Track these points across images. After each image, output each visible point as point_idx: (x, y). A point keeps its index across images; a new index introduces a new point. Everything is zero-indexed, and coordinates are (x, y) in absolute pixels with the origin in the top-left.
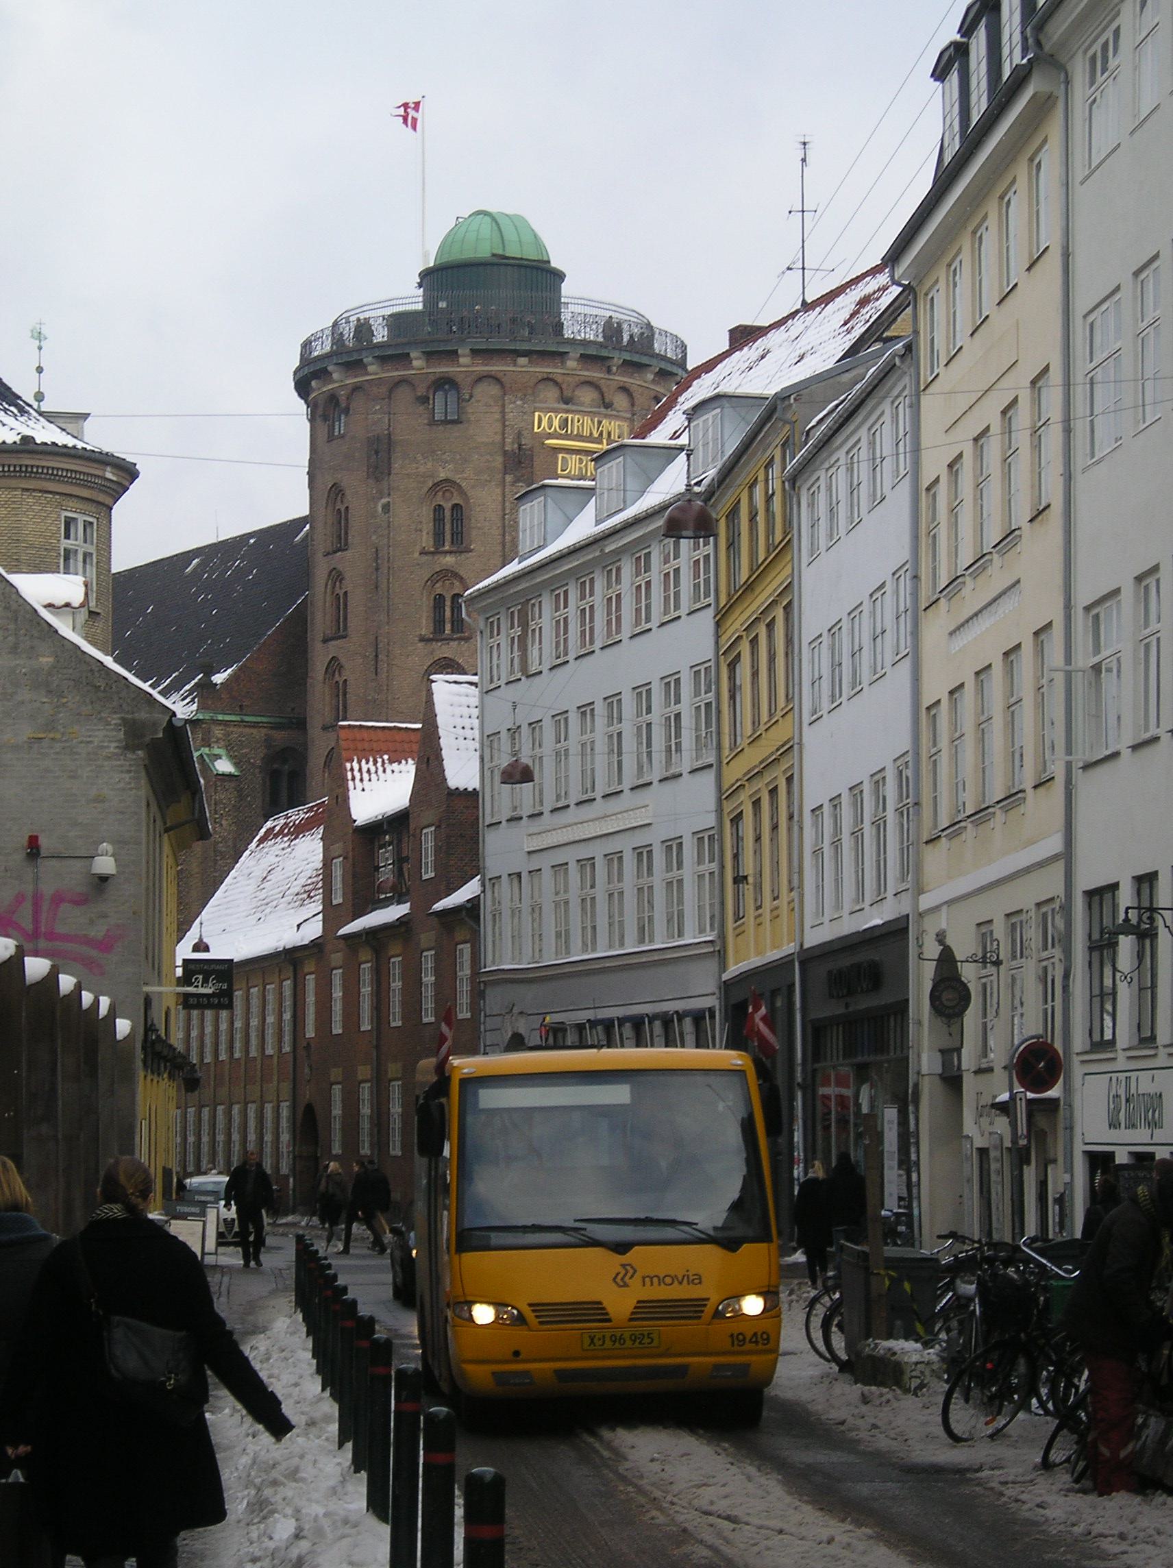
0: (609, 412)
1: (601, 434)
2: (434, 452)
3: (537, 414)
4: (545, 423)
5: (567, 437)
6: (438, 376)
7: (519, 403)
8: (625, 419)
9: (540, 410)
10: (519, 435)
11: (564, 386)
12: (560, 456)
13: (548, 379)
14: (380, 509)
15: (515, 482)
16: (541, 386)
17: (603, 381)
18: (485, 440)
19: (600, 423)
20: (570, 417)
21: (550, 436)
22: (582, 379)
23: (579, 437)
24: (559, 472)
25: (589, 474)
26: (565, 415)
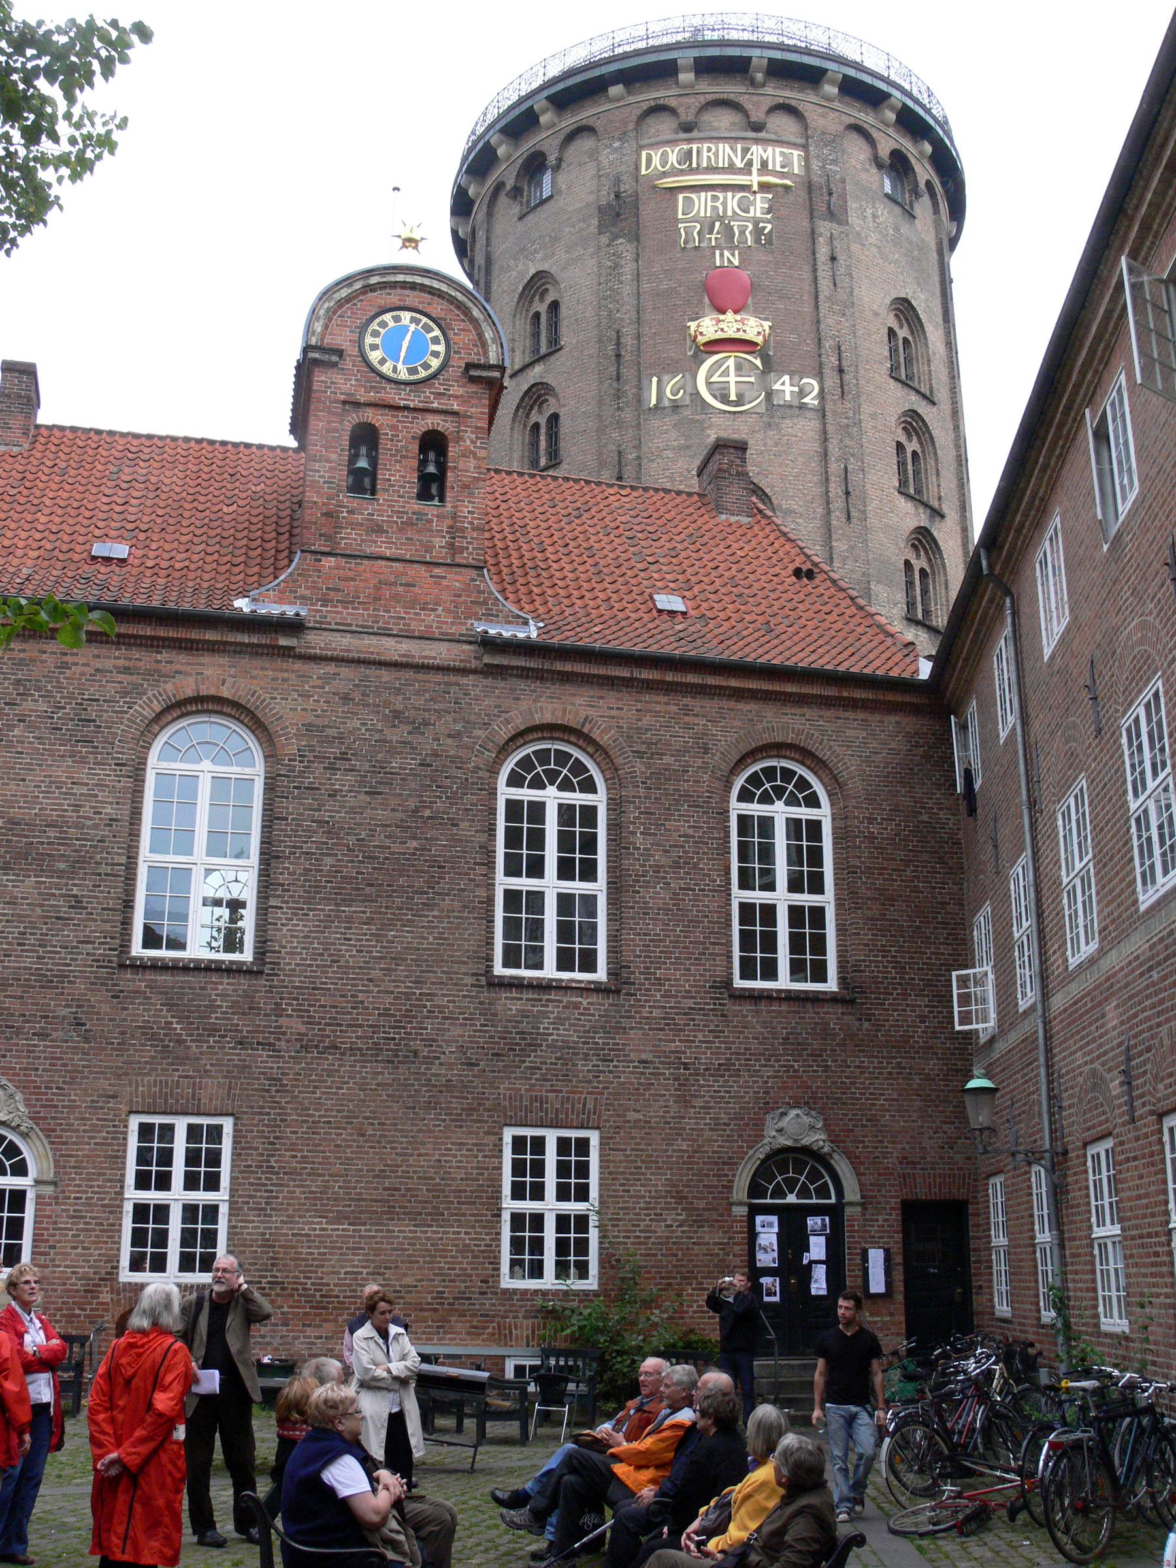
0: (762, 135)
1: (750, 164)
2: (524, 248)
3: (644, 154)
4: (656, 160)
5: (691, 171)
8: (794, 145)
9: (651, 146)
12: (681, 197)
15: (613, 240)
16: (650, 120)
17: (747, 96)
18: (578, 205)
19: (745, 151)
20: (695, 147)
21: (664, 174)
22: (710, 97)
24: (680, 216)
25: (730, 213)
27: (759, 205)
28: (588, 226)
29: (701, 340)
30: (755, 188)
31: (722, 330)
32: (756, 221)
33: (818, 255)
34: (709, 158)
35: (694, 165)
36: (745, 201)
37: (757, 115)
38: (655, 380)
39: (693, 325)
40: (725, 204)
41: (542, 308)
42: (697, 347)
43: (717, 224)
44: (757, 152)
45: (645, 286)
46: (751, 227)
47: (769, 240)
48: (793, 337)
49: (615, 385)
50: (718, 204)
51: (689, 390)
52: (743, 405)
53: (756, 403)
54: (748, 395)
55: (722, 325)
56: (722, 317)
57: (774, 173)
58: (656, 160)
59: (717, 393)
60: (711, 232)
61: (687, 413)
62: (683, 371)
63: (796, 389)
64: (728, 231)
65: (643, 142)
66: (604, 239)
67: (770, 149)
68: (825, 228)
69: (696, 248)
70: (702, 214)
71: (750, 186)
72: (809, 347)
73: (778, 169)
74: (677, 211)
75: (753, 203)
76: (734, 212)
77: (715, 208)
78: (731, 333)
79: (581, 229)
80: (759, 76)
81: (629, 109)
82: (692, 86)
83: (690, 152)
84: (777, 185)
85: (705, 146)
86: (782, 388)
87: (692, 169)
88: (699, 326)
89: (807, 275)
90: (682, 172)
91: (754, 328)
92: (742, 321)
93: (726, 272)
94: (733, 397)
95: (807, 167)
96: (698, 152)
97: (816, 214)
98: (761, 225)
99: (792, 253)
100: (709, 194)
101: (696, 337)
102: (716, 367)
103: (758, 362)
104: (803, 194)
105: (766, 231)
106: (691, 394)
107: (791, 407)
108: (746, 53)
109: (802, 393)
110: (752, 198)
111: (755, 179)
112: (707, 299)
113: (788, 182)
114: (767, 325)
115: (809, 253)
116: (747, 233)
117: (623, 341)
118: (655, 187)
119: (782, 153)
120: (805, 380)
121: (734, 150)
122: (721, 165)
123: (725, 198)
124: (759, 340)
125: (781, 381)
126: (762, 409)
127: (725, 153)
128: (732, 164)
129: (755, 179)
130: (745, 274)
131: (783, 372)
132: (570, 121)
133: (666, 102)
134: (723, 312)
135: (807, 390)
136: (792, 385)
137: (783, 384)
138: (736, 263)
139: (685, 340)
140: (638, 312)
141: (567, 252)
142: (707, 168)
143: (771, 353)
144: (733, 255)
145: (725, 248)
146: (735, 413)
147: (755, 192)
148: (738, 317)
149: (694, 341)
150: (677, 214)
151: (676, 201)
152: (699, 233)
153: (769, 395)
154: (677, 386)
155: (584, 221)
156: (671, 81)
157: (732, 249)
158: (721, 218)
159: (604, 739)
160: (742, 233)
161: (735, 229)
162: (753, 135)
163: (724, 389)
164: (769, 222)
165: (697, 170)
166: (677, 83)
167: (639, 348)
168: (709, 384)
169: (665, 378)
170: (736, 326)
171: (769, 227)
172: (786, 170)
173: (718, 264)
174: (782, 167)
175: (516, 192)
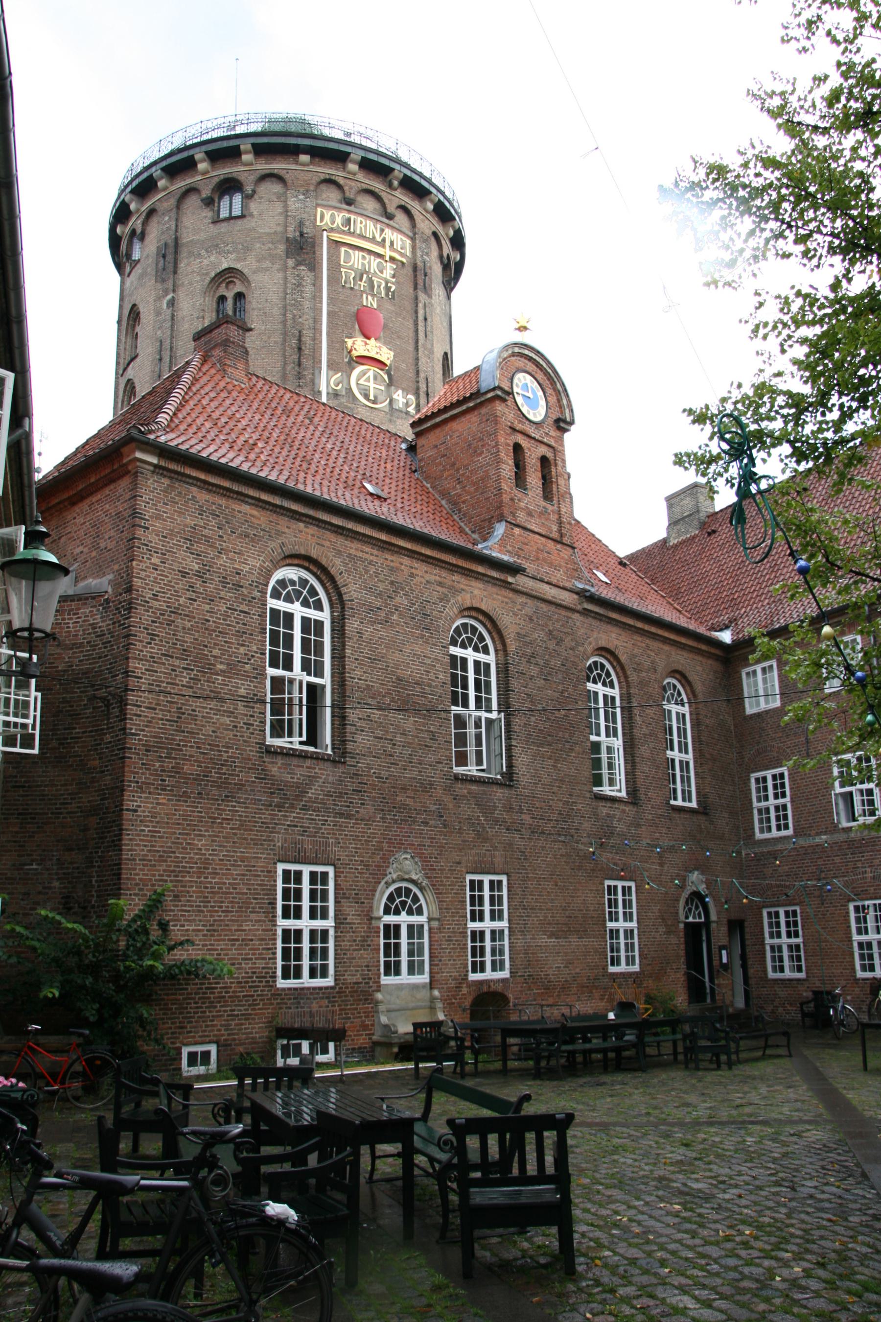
0: (391, 223)
2: (217, 245)
3: (319, 210)
5: (350, 233)
6: (222, 177)
7: (301, 197)
10: (301, 224)
11: (346, 188)
13: (330, 182)
14: (165, 306)
16: (323, 187)
18: (268, 230)
20: (353, 217)
22: (365, 186)
23: (362, 237)
26: (347, 215)
28: (276, 248)
29: (355, 353)
30: (387, 259)
37: (350, 194)
39: (349, 342)
40: (369, 263)
41: (230, 295)
42: (351, 358)
44: (389, 234)
49: (297, 368)
53: (383, 405)
55: (368, 347)
60: (361, 280)
61: (343, 400)
64: (371, 282)
65: (320, 202)
66: (291, 263)
68: (422, 297)
69: (352, 289)
72: (411, 374)
75: (385, 268)
77: (363, 264)
78: (372, 354)
79: (269, 249)
80: (396, 183)
81: (311, 175)
82: (355, 174)
83: (349, 220)
89: (410, 324)
90: (343, 232)
91: (386, 355)
103: (386, 377)
108: (393, 165)
111: (388, 253)
112: (357, 326)
113: (404, 260)
117: (303, 339)
124: (388, 363)
126: (387, 410)
127: (370, 228)
128: (374, 238)
132: (264, 166)
133: (337, 178)
134: (369, 338)
138: (375, 306)
141: (258, 261)
155: (273, 243)
156: (340, 166)
157: (373, 296)
159: (623, 658)
160: (379, 287)
162: (386, 221)
165: (352, 234)
166: (344, 168)
175: (209, 202)
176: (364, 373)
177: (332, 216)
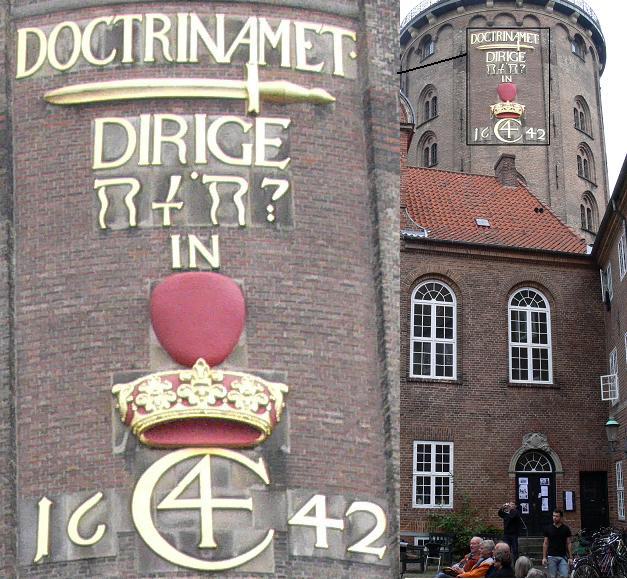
1: (243, 54)
3: (22, 34)
4: (48, 49)
5: (121, 70)
8: (336, 17)
9: (37, 17)
12: (99, 124)
19: (234, 28)
20: (128, 20)
21: (65, 77)
24: (98, 164)
25: (201, 158)
27: (261, 140)
29: (141, 421)
30: (254, 105)
31: (185, 400)
32: (256, 175)
33: (384, 245)
34: (158, 42)
35: (127, 58)
36: (233, 134)
38: (45, 505)
39: (124, 391)
40: (190, 139)
42: (134, 437)
43: (175, 181)
44: (258, 30)
45: (26, 310)
46: (244, 186)
47: (283, 216)
48: (334, 417)
50: (177, 139)
51: (117, 525)
52: (229, 557)
53: (257, 551)
54: (239, 536)
55: (185, 391)
56: (184, 374)
57: (294, 74)
58: (48, 49)
59: (175, 533)
60: (162, 198)
62: (104, 487)
63: (339, 524)
64: (198, 194)
65: (20, 10)
67: (285, 25)
70: (144, 160)
71: (243, 102)
73: (302, 65)
74: (91, 152)
75: (250, 137)
76: (210, 155)
77: (170, 147)
78: (203, 408)
83: (118, 30)
84: (299, 100)
85: (150, 17)
86: (309, 521)
87: (123, 67)
88: (136, 392)
90: (101, 73)
92: (227, 383)
93: (193, 278)
94: (208, 541)
95: (363, 61)
96: (135, 30)
97: (380, 159)
98: (266, 182)
99: (330, 241)
100: (159, 118)
101: (130, 416)
102: (171, 477)
103: (260, 468)
104: (354, 118)
105: (276, 196)
106: (121, 535)
107: (328, 561)
109: (351, 533)
110: (247, 126)
111: (252, 87)
112: (153, 337)
114: (278, 389)
115: (367, 240)
116: (237, 198)
118: (46, 103)
119: (310, 33)
120: (356, 506)
121: (211, 27)
122: (182, 58)
123: (192, 127)
124: (263, 421)
125: (307, 507)
126: (269, 566)
128: (205, 57)
129: (252, 87)
130: (233, 285)
131: (314, 488)
134: (188, 364)
135: (362, 524)
136: (330, 515)
137: (312, 513)
138: (215, 262)
139: (107, 421)
140: (11, 365)
142: (153, 64)
143: (287, 449)
144: (208, 245)
145: (192, 230)
146: (211, 573)
147: (253, 114)
148: (219, 374)
149: (127, 423)
150: (90, 159)
151: (89, 133)
152: (137, 199)
153: (284, 536)
154: (92, 518)
157: (205, 233)
158: (181, 169)
160: (227, 199)
161: (213, 190)
163: (190, 523)
164: (282, 175)
165: (133, 69)
167: (12, 440)
168: (157, 513)
169: (67, 500)
170: (217, 391)
171: (283, 186)
172: (317, 68)
173: (176, 264)
174: (311, 61)
176: (177, 472)
177: (65, 37)
